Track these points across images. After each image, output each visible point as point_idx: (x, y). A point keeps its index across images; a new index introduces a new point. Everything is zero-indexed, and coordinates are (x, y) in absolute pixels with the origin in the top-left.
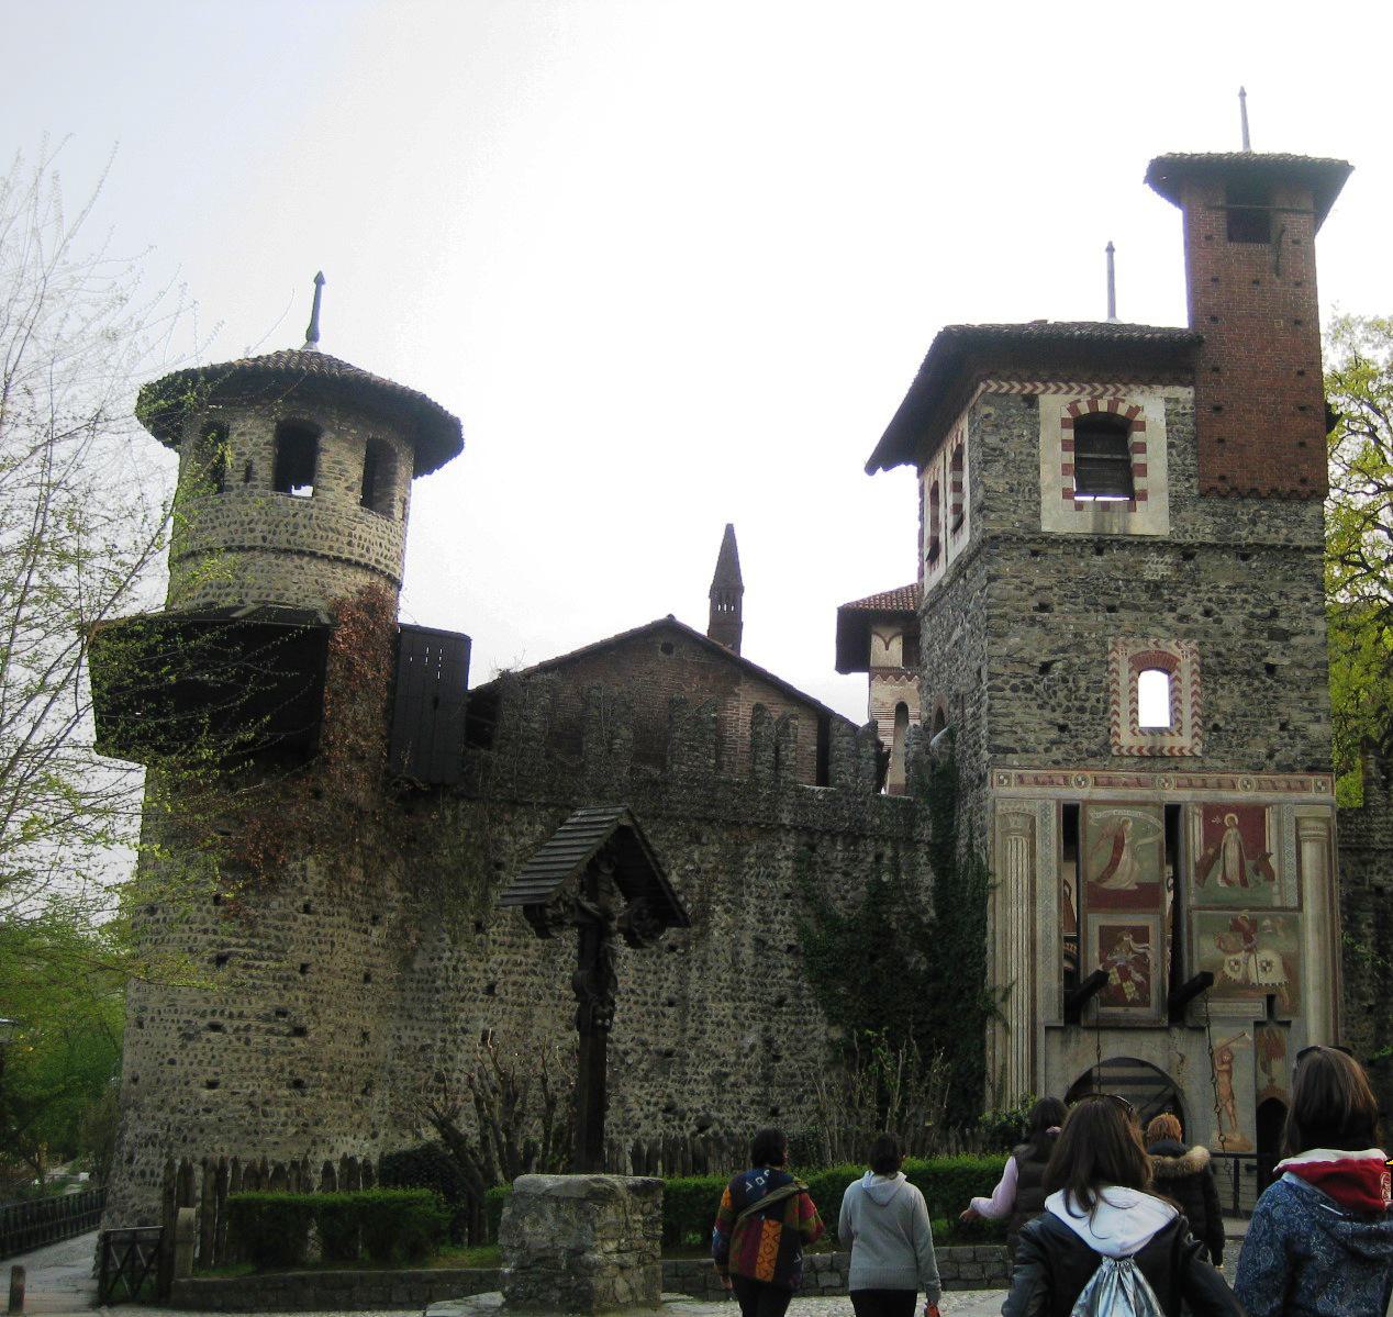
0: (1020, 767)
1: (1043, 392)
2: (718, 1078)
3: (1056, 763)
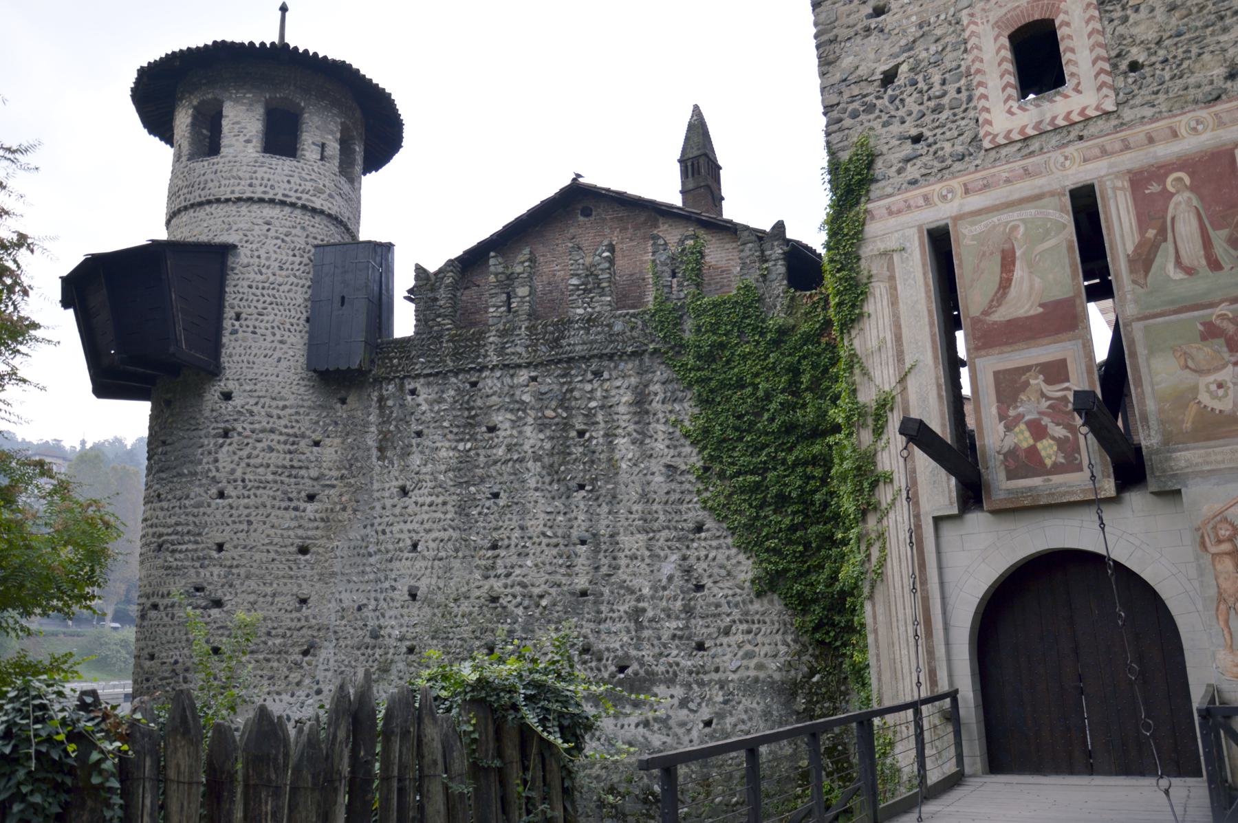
2: (637, 613)
3: (914, 182)
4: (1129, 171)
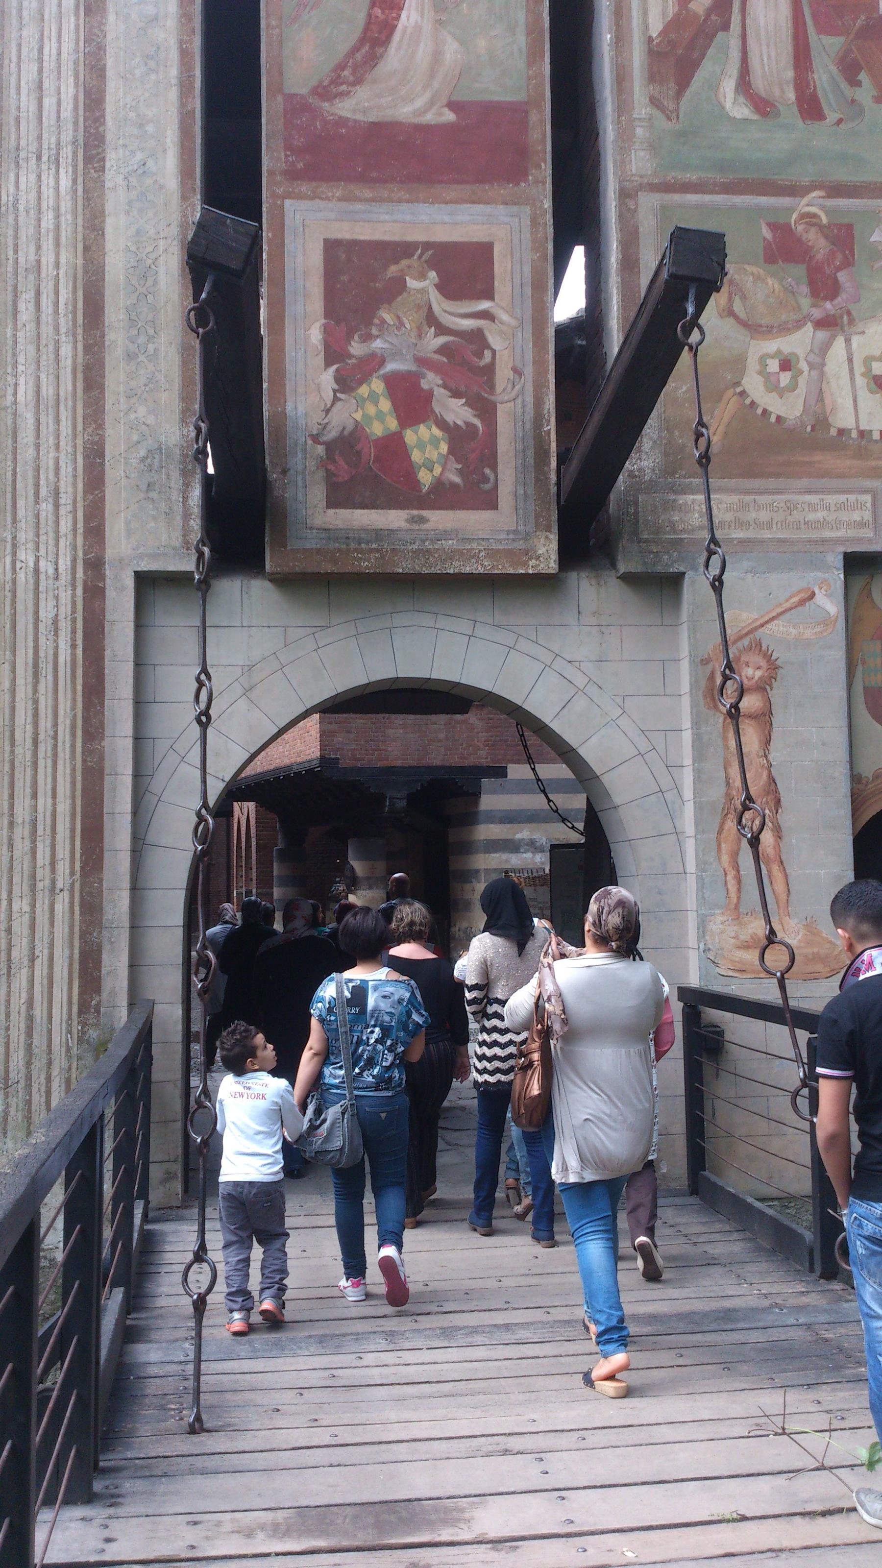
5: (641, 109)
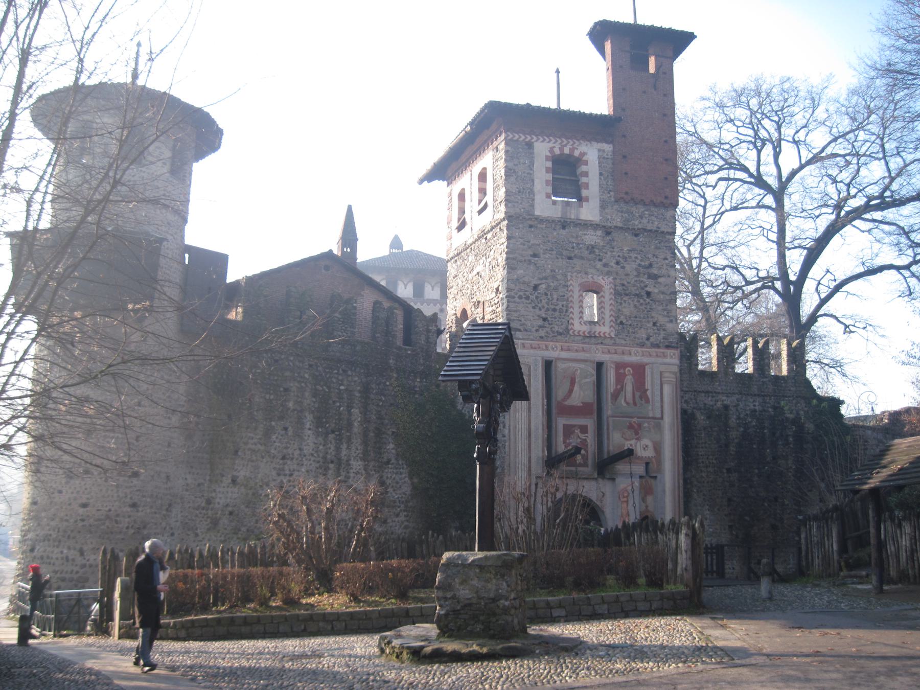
0: (523, 339)
1: (536, 141)
3: (541, 337)
4: (615, 362)
5: (610, 404)
